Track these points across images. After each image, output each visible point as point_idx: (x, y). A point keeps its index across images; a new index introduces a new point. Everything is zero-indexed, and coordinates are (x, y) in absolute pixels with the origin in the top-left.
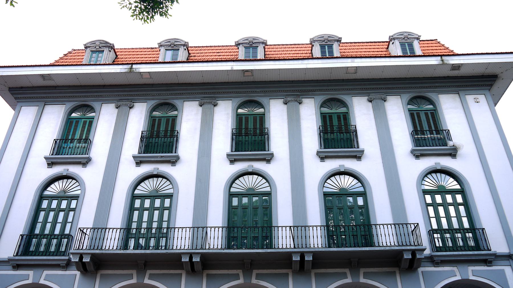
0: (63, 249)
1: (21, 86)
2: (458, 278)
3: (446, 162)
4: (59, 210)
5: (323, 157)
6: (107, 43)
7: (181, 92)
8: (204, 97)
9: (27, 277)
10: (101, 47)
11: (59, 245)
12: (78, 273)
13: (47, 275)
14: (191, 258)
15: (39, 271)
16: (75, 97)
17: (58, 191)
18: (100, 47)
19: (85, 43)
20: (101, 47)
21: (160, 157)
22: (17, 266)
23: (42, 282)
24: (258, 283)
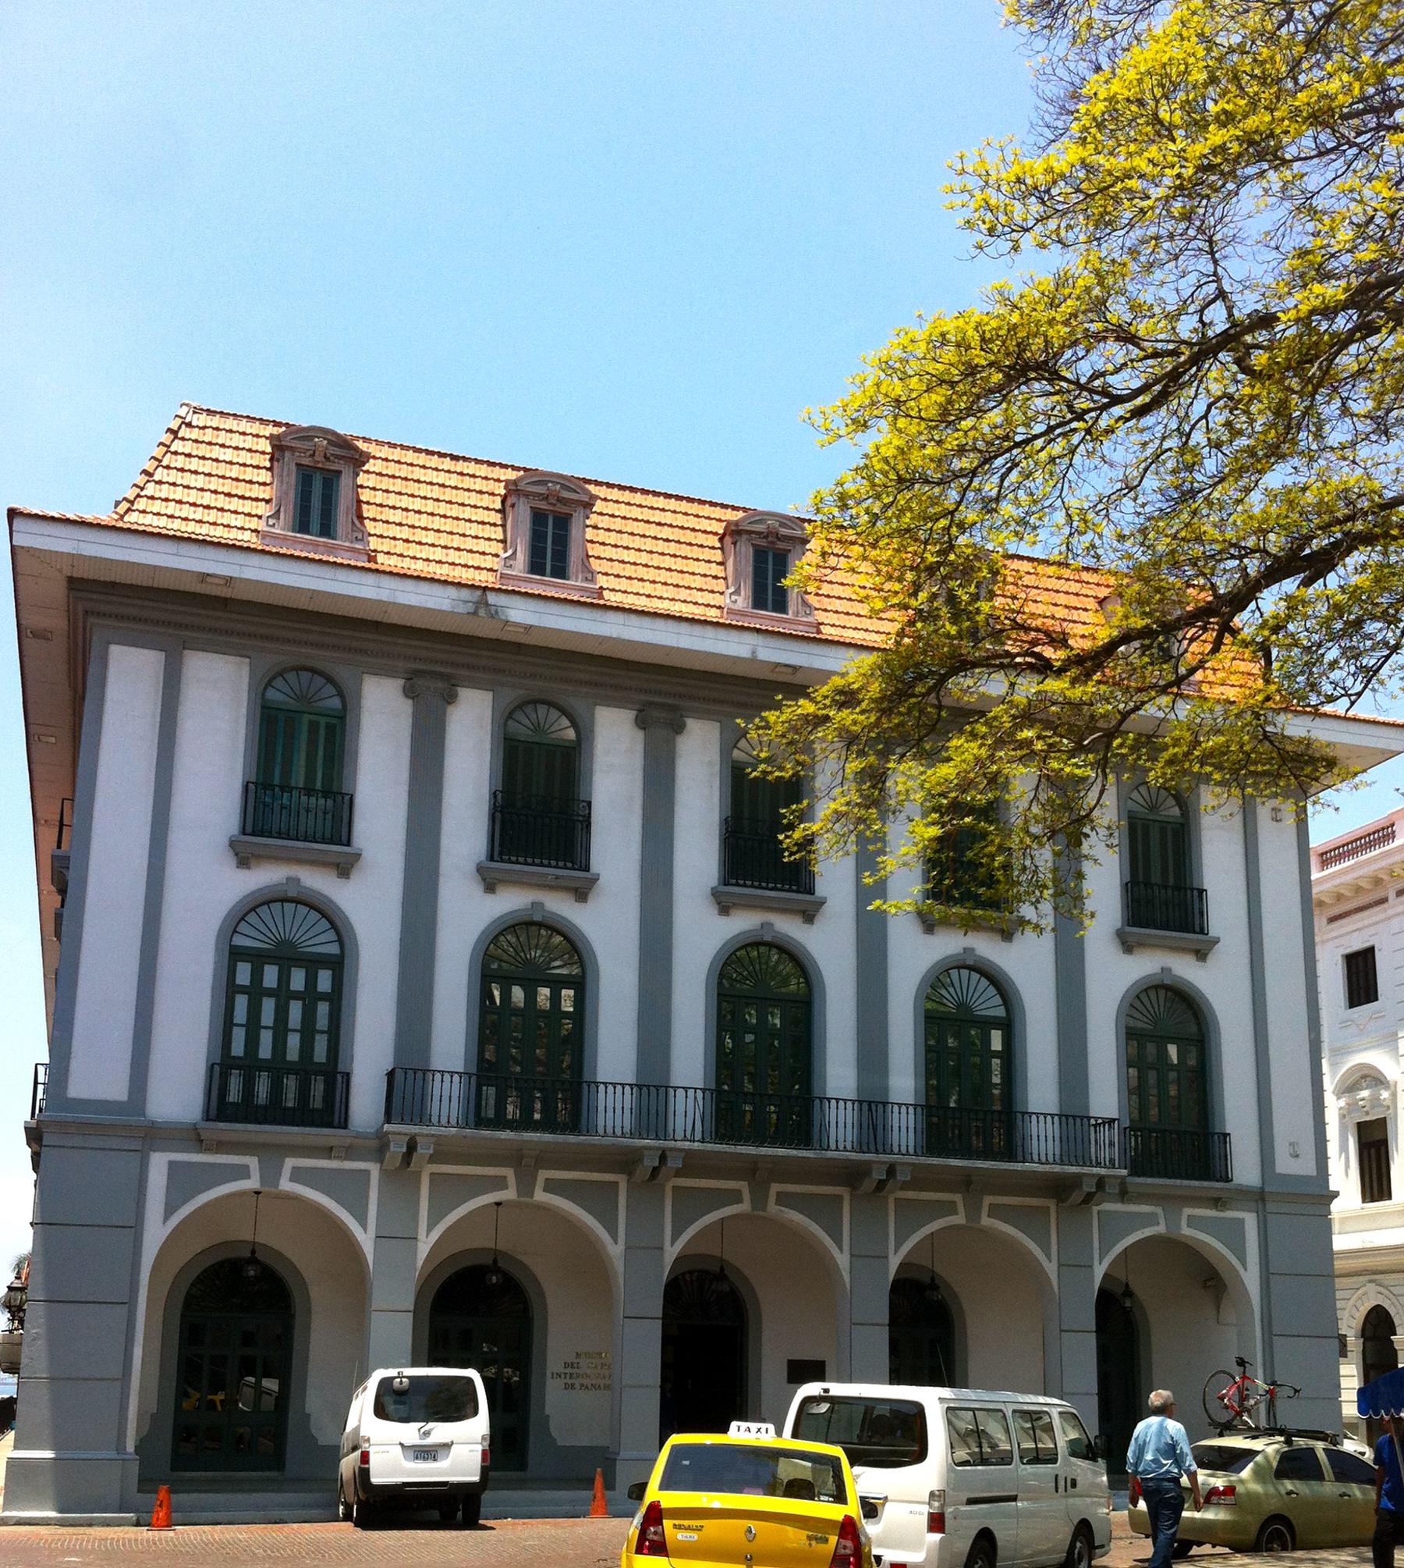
0: (317, 1100)
2: (1160, 1229)
3: (1185, 969)
4: (283, 995)
5: (929, 925)
8: (651, 703)
9: (243, 1173)
11: (304, 1093)
13: (295, 1169)
22: (222, 1147)
23: (286, 1185)
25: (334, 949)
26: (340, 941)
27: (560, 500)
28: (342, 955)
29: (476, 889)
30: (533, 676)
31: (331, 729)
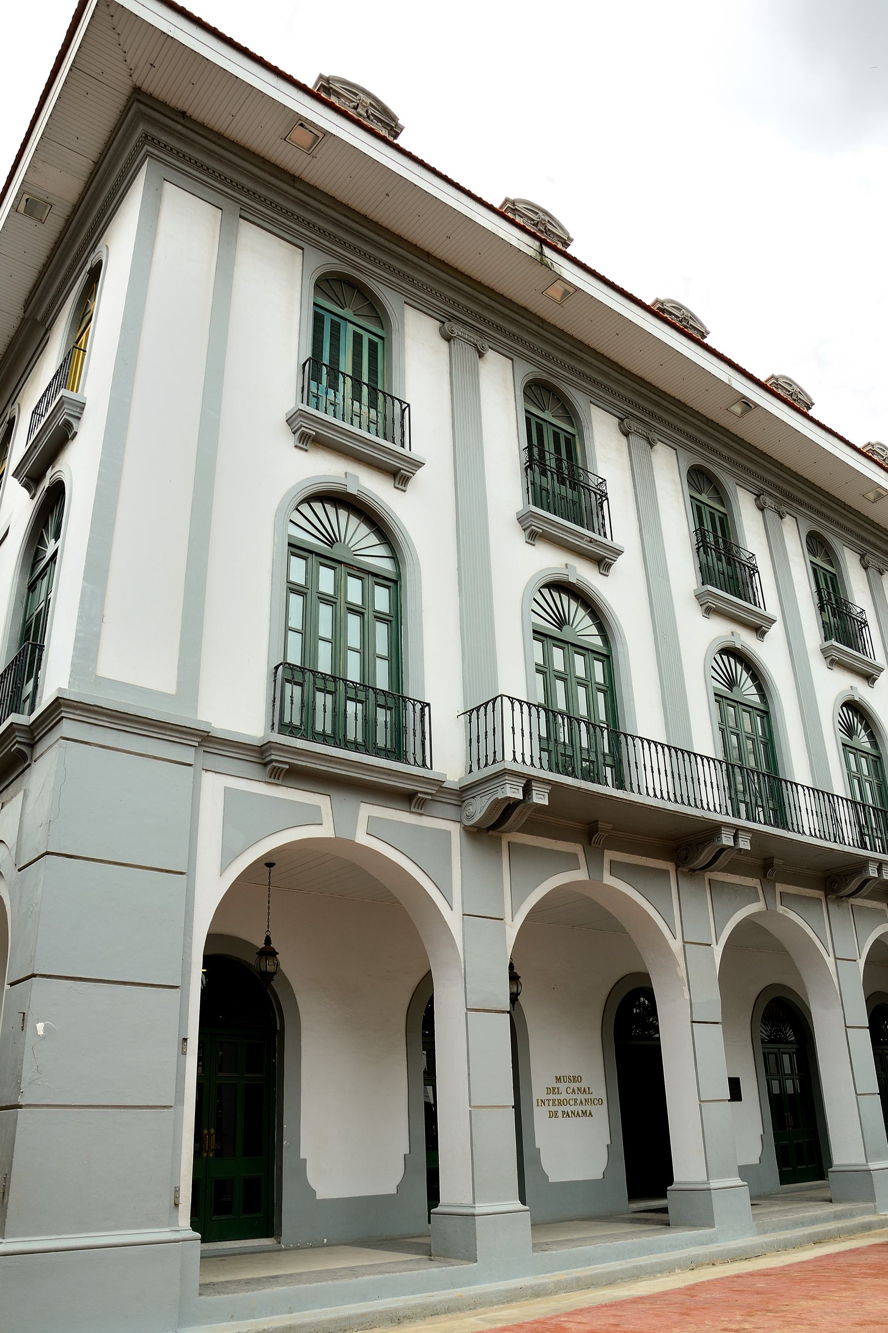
1: (184, 109)
6: (385, 111)
7: (594, 375)
8: (631, 414)
10: (372, 117)
11: (369, 724)
12: (455, 830)
14: (736, 838)
15: (346, 801)
16: (343, 244)
17: (350, 546)
18: (368, 117)
19: (327, 75)
20: (372, 117)
21: (588, 539)
23: (362, 838)
24: (786, 914)
25: (386, 566)
26: (395, 555)
27: (547, 231)
28: (399, 575)
29: (519, 537)
30: (547, 356)
31: (373, 346)
